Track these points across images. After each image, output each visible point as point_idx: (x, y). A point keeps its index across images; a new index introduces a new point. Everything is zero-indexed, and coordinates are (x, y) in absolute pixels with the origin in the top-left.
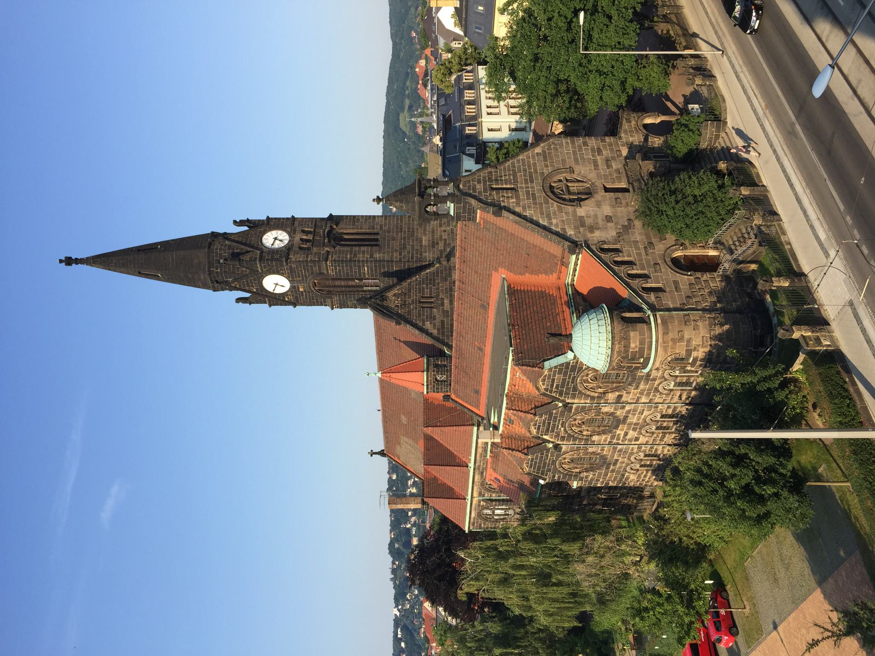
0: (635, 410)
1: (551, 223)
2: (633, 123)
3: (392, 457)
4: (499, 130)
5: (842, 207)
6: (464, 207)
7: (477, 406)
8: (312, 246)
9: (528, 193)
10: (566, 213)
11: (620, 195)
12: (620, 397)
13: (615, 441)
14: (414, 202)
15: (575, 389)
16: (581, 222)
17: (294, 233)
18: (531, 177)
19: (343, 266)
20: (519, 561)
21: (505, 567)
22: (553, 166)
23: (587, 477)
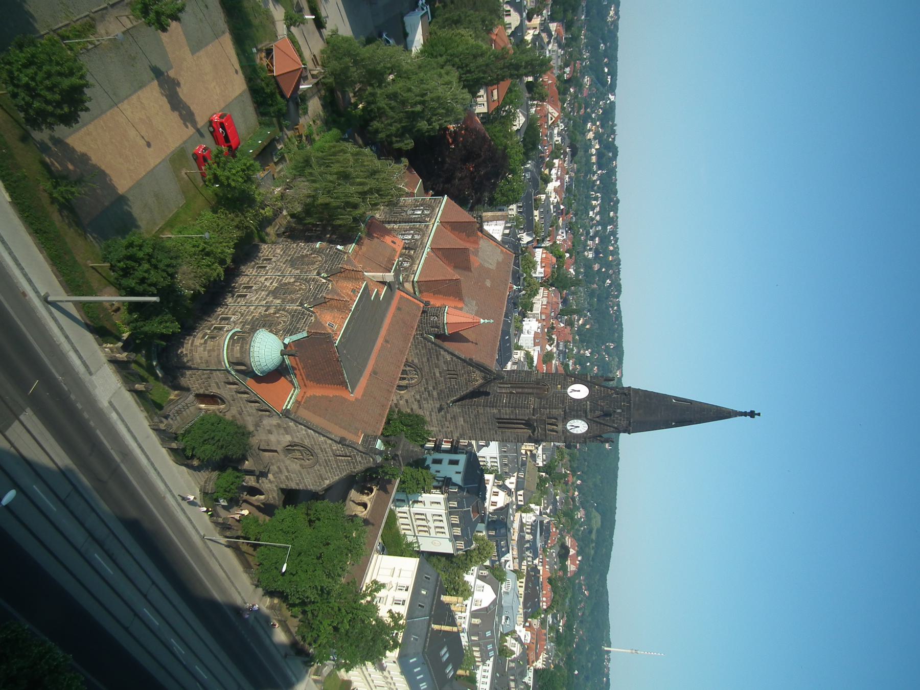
0: (260, 300)
1: (306, 431)
2: (271, 497)
3: (508, 251)
4: (432, 503)
5: (98, 432)
6: (369, 445)
7: (402, 297)
8: (545, 421)
9: (326, 453)
10: (298, 437)
11: (267, 448)
12: (266, 311)
13: (281, 278)
14: (403, 450)
15: (293, 316)
16: (287, 430)
17: (563, 431)
18: (327, 464)
19: (522, 403)
20: (360, 189)
21: (372, 183)
22: (315, 470)
23: (308, 251)
